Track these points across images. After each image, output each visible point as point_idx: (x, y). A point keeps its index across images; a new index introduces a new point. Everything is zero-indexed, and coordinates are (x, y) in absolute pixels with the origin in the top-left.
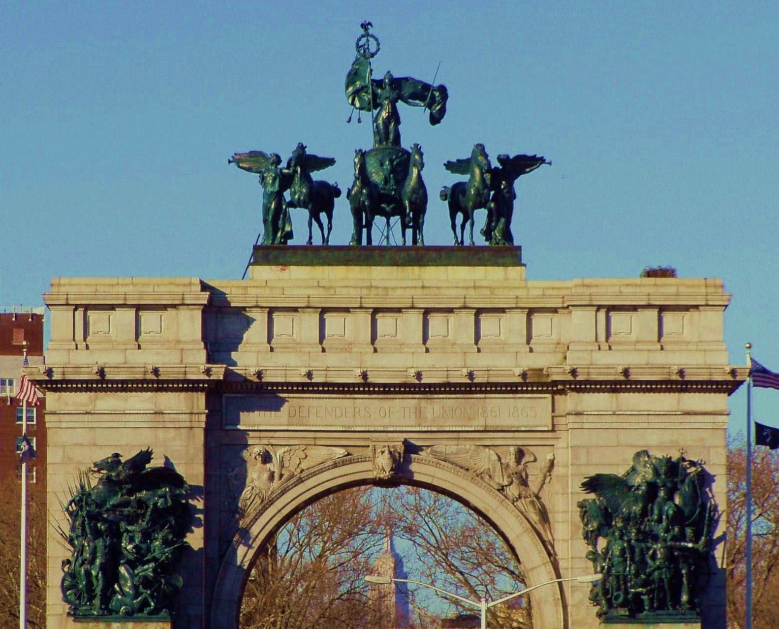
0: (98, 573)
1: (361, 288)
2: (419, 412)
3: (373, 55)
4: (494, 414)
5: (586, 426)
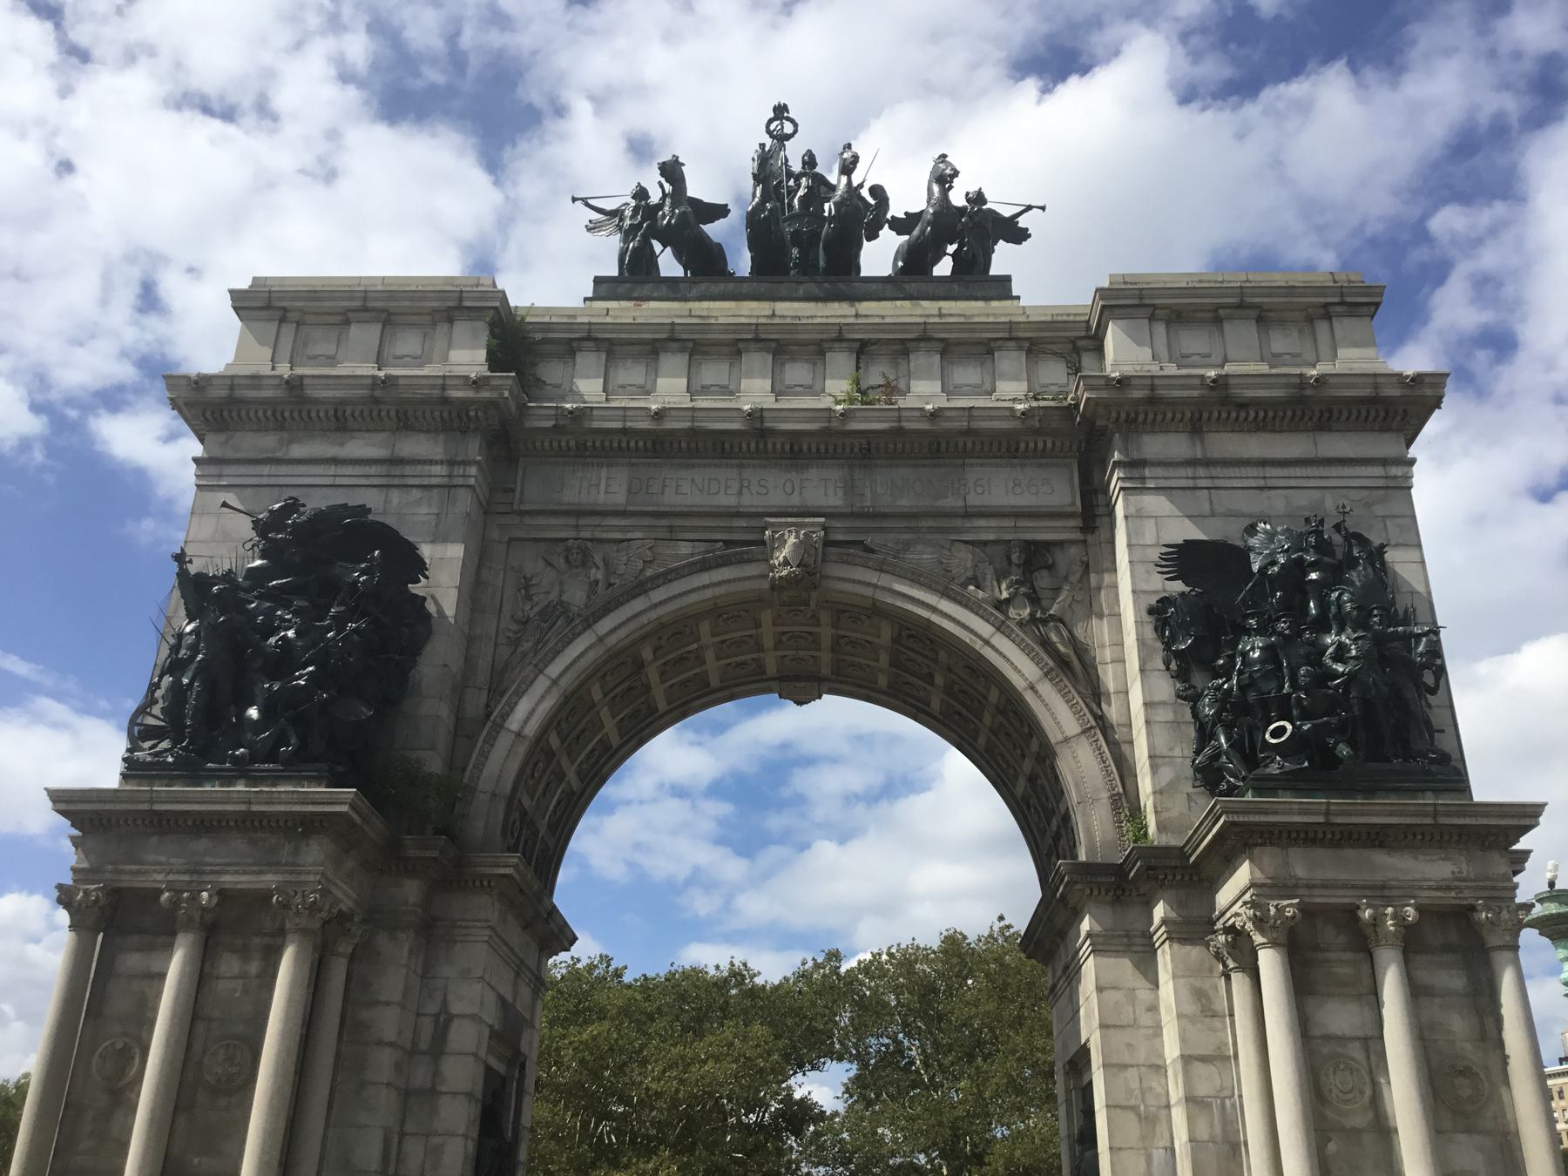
1: (758, 317)
2: (850, 488)
3: (789, 137)
4: (979, 490)
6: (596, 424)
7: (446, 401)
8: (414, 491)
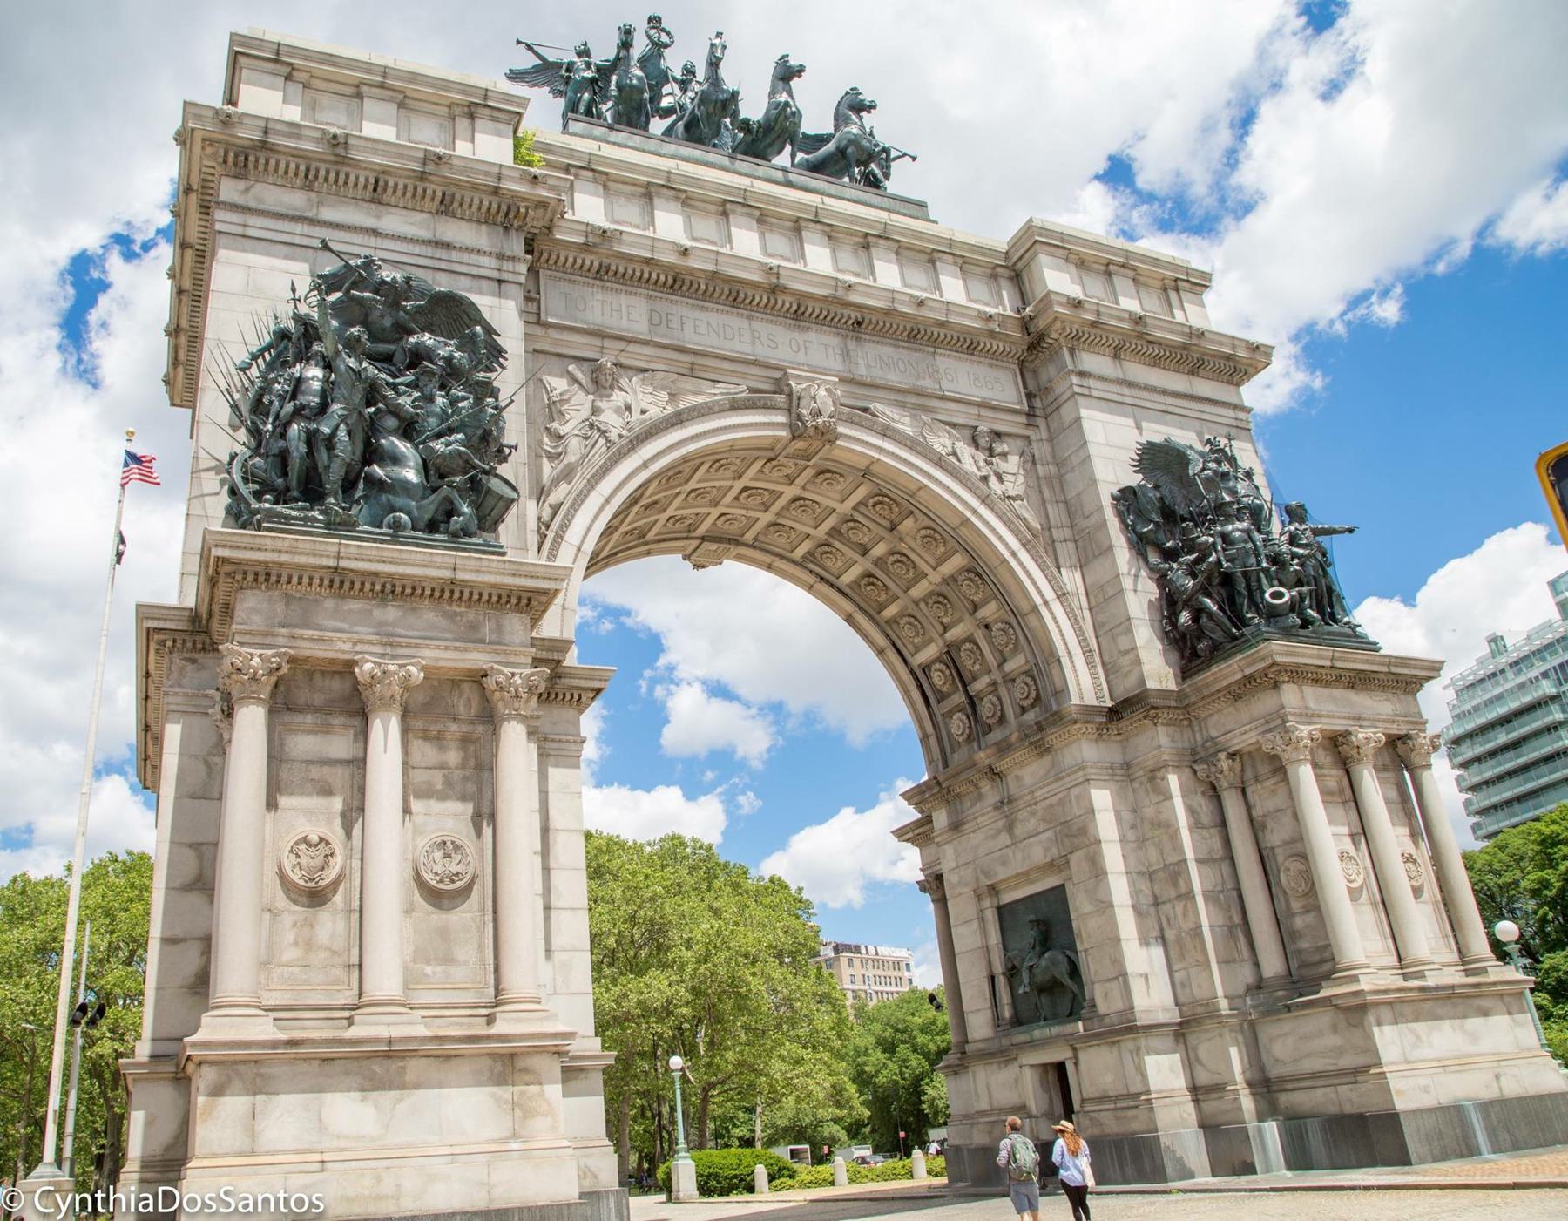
0: (337, 428)
5: (1095, 393)
6: (625, 250)
7: (496, 191)
8: (462, 278)
